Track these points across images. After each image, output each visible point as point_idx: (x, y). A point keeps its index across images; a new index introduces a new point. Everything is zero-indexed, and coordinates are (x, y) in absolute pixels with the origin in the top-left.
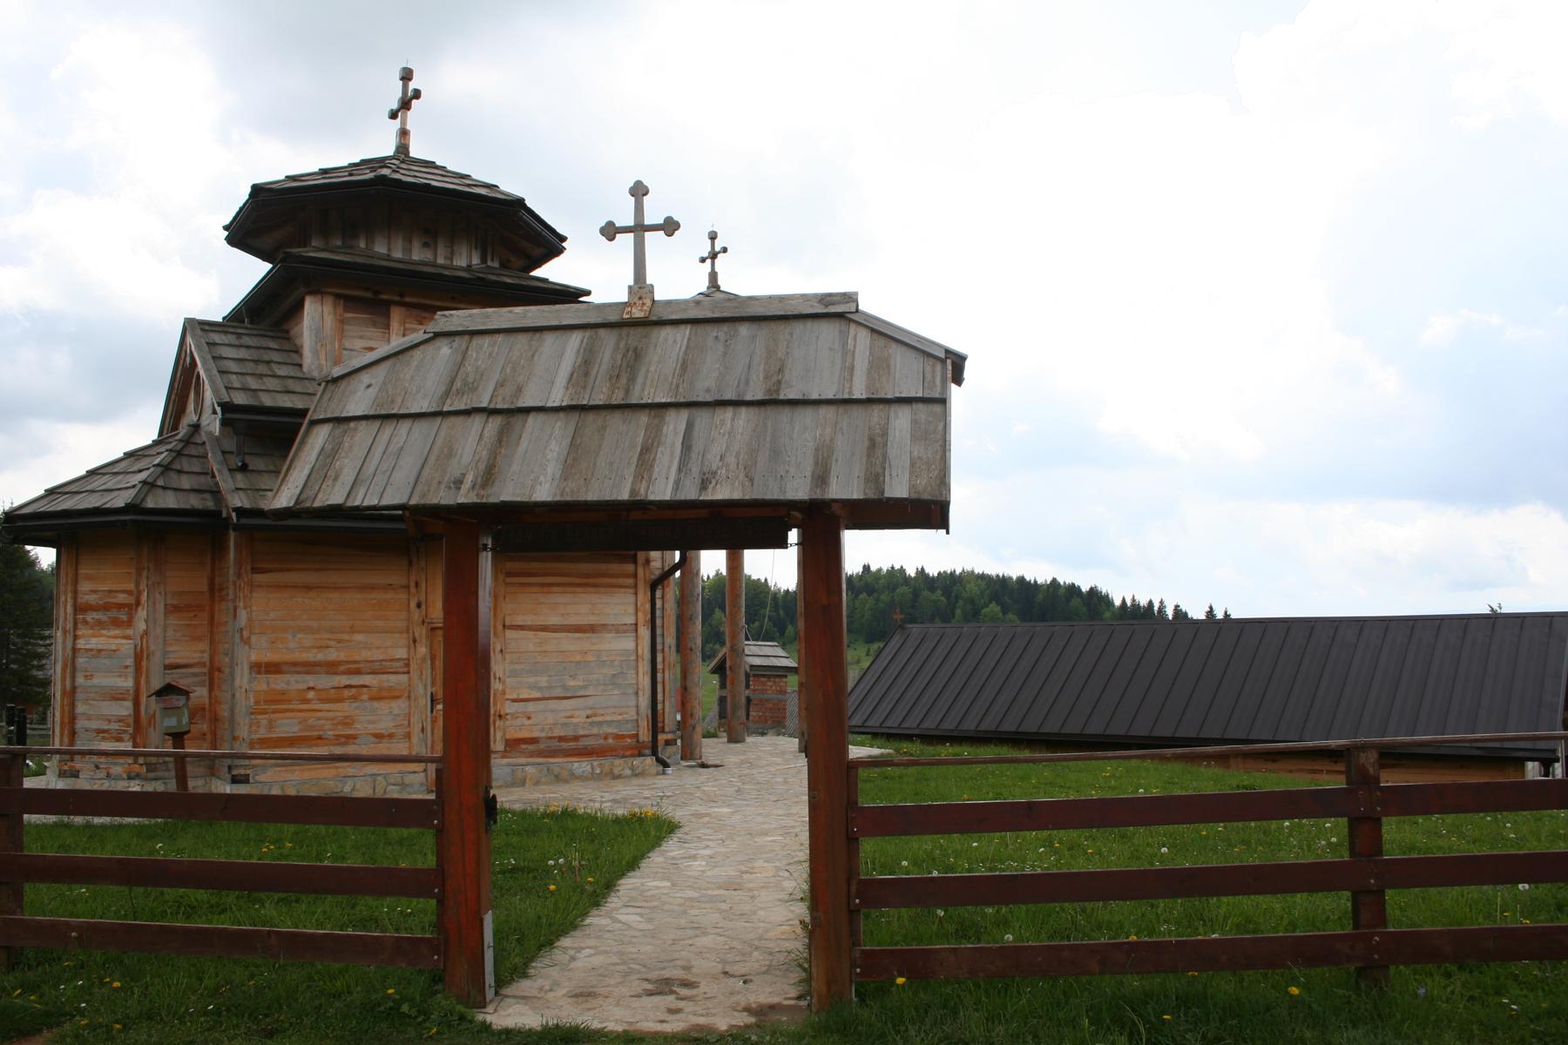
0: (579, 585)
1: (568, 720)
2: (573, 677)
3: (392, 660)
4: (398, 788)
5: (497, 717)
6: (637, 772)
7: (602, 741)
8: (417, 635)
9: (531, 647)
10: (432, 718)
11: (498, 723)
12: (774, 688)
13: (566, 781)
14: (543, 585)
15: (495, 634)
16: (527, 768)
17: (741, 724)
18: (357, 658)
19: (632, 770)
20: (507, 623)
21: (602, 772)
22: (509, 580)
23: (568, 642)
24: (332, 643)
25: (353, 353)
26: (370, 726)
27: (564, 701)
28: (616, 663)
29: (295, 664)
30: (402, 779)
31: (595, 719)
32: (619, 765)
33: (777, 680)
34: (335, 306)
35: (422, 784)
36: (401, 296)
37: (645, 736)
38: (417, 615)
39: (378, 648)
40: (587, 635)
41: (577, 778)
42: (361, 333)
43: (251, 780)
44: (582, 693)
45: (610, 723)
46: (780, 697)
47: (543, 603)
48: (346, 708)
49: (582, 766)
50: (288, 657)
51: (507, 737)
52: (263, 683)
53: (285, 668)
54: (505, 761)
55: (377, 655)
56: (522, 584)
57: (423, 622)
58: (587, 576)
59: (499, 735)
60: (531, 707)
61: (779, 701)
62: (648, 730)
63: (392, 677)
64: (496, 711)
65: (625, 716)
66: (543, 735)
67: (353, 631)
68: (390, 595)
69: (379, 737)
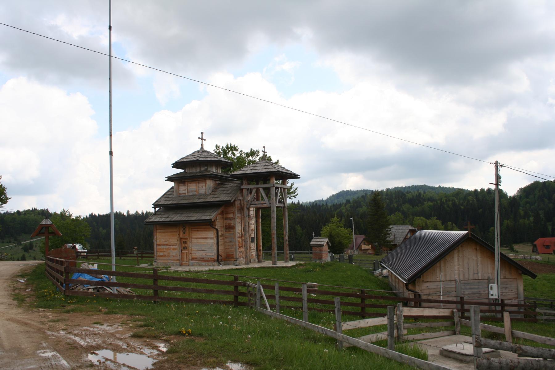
2: (203, 247)
7: (208, 259)
9: (196, 242)
13: (201, 266)
14: (198, 230)
20: (192, 237)
22: (192, 230)
29: (162, 244)
32: (210, 263)
33: (320, 248)
37: (216, 259)
38: (178, 236)
44: (204, 250)
45: (210, 256)
48: (169, 251)
49: (204, 263)
50: (161, 243)
52: (159, 247)
60: (196, 252)
63: (175, 247)
67: (169, 239)
69: (173, 256)
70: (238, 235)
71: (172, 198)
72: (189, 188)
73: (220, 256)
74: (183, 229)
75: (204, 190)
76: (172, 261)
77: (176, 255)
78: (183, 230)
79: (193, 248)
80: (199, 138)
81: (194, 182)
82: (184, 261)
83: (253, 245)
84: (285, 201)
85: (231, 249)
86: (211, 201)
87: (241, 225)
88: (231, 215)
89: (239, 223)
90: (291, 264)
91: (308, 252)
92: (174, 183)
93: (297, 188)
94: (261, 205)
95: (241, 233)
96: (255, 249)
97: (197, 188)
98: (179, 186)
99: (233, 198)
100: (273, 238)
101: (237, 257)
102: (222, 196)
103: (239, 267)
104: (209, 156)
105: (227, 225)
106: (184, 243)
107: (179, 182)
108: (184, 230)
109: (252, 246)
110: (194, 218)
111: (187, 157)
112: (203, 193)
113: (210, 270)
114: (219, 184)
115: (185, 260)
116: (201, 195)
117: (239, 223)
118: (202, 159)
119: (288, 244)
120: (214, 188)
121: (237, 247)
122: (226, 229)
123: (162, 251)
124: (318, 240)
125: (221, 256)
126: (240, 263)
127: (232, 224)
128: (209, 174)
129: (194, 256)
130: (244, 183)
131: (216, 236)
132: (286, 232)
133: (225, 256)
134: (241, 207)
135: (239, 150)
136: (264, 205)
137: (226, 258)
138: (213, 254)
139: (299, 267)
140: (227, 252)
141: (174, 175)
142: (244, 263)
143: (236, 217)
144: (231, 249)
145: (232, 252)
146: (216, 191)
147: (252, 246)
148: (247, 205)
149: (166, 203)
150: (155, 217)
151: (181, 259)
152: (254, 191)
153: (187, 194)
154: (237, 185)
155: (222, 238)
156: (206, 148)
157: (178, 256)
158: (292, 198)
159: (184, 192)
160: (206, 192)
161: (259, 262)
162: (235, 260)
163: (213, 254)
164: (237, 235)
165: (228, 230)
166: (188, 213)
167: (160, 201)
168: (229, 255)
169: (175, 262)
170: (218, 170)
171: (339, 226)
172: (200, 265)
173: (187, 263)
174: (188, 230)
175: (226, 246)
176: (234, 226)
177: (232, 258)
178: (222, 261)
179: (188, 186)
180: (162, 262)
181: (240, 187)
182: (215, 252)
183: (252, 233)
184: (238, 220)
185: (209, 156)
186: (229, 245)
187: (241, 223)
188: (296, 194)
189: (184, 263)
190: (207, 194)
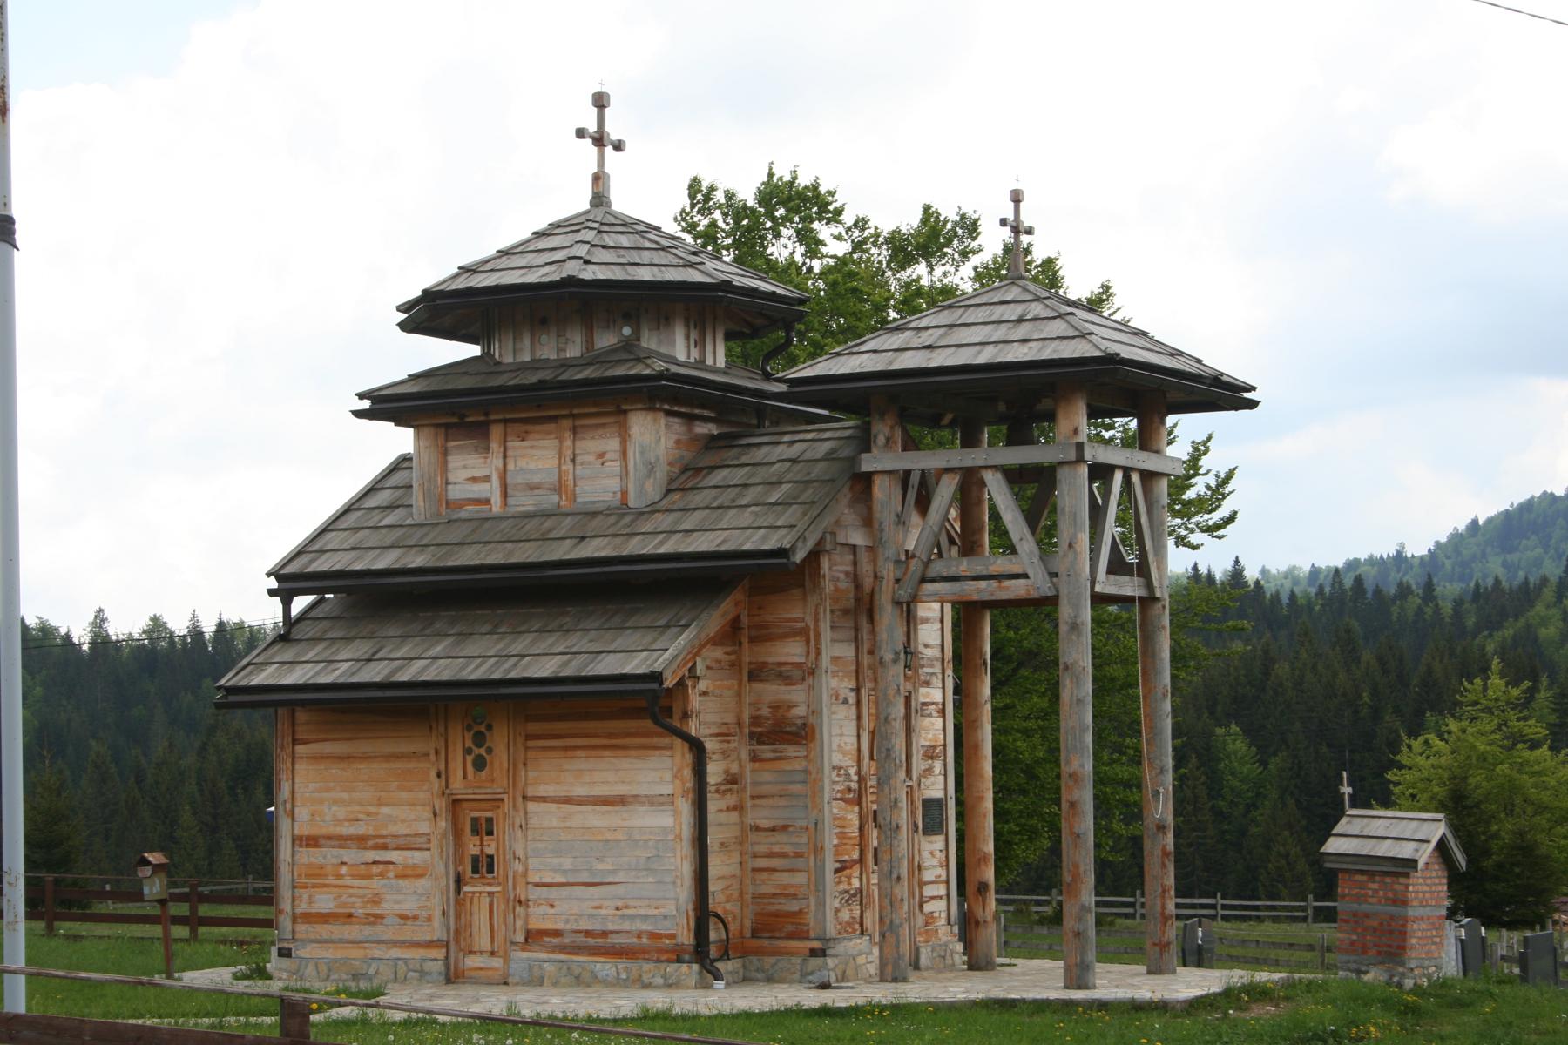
0: (605, 747)
1: (595, 912)
2: (600, 859)
3: (416, 835)
4: (417, 974)
5: (517, 904)
6: (670, 982)
7: (635, 940)
8: (437, 807)
9: (555, 822)
10: (457, 902)
11: (518, 909)
12: (1381, 893)
13: (589, 986)
14: (566, 748)
15: (514, 806)
16: (546, 965)
17: (1155, 944)
18: (384, 832)
19: (665, 980)
20: (530, 792)
21: (628, 978)
22: (531, 743)
23: (596, 818)
24: (362, 816)
25: (457, 487)
26: (397, 907)
27: (591, 888)
28: (650, 843)
29: (330, 838)
30: (421, 966)
31: (626, 912)
33: (1388, 880)
34: (436, 435)
35: (440, 973)
36: (486, 414)
37: (686, 938)
38: (436, 785)
39: (403, 821)
40: (617, 808)
41: (600, 982)
42: (463, 463)
43: (293, 955)
44: (611, 879)
45: (645, 918)
46: (1392, 909)
47: (568, 770)
48: (376, 884)
49: (605, 967)
50: (324, 831)
51: (530, 927)
52: (306, 856)
53: (322, 842)
54: (526, 955)
55: (401, 829)
56: (545, 749)
57: (443, 794)
58: (610, 736)
59: (519, 923)
60: (554, 893)
61: (1392, 918)
62: (689, 930)
63: (417, 854)
64: (515, 896)
65: (662, 910)
66: (568, 927)
67: (380, 804)
68: (411, 765)
69: (404, 917)
70: (834, 783)
71: (398, 533)
72: (511, 466)
73: (712, 921)
74: (469, 737)
75: (614, 484)
76: (395, 953)
77: (424, 913)
78: (469, 743)
79: (533, 862)
80: (581, 133)
81: (552, 426)
82: (471, 952)
83: (931, 853)
84: (1151, 557)
85: (786, 878)
86: (662, 550)
87: (859, 717)
88: (791, 652)
89: (845, 701)
90: (1189, 984)
91: (1303, 909)
92: (410, 431)
93: (1230, 474)
94: (994, 583)
95: (858, 773)
96: (947, 882)
97: (568, 467)
98: (445, 453)
99: (802, 537)
100: (1073, 805)
101: (831, 930)
102: (730, 518)
103: (837, 998)
104: (646, 257)
105: (766, 712)
106: (476, 831)
107: (447, 426)
108: (479, 746)
109: (925, 854)
110: (545, 668)
111: (504, 262)
112: (608, 497)
113: (647, 1017)
114: (713, 438)
115: (484, 942)
116: (594, 514)
117: (845, 701)
118: (601, 274)
119: (1171, 848)
120: (676, 470)
121: (830, 865)
122: (758, 738)
123: (331, 881)
124: (1378, 827)
125: (722, 920)
126: (849, 972)
127: (790, 707)
128: (647, 371)
129: (541, 918)
130: (881, 440)
131: (689, 785)
132: (1162, 771)
133: (748, 924)
134: (858, 600)
135: (848, 218)
136: (1014, 581)
137: (755, 934)
138: (670, 909)
139: (1247, 1010)
140: (762, 896)
141: (414, 378)
142: (873, 969)
143: (825, 661)
144: (786, 878)
145: (794, 896)
146: (692, 489)
147: (928, 861)
148: (897, 581)
149: (358, 567)
150: (288, 654)
151: (457, 942)
152: (946, 490)
153: (496, 507)
154: (833, 451)
155: (731, 800)
156: (623, 202)
157: (437, 920)
158: (1196, 538)
159: (479, 490)
160: (624, 493)
161: (973, 966)
162: (814, 953)
163: (670, 909)
164: (827, 782)
165: (766, 751)
166: (502, 630)
167: (322, 552)
168: (777, 915)
169: (415, 954)
170: (709, 348)
171: (1516, 739)
172: (580, 981)
173: (497, 963)
174: (500, 740)
175: (755, 856)
176: (811, 720)
177: (792, 936)
178: (725, 955)
179: (505, 457)
180: (328, 953)
181: (853, 461)
182: (684, 893)
183: (929, 771)
184: (835, 683)
185: (646, 257)
186: (776, 849)
187: (858, 703)
188: (1223, 512)
189: (472, 962)
190: (631, 504)
